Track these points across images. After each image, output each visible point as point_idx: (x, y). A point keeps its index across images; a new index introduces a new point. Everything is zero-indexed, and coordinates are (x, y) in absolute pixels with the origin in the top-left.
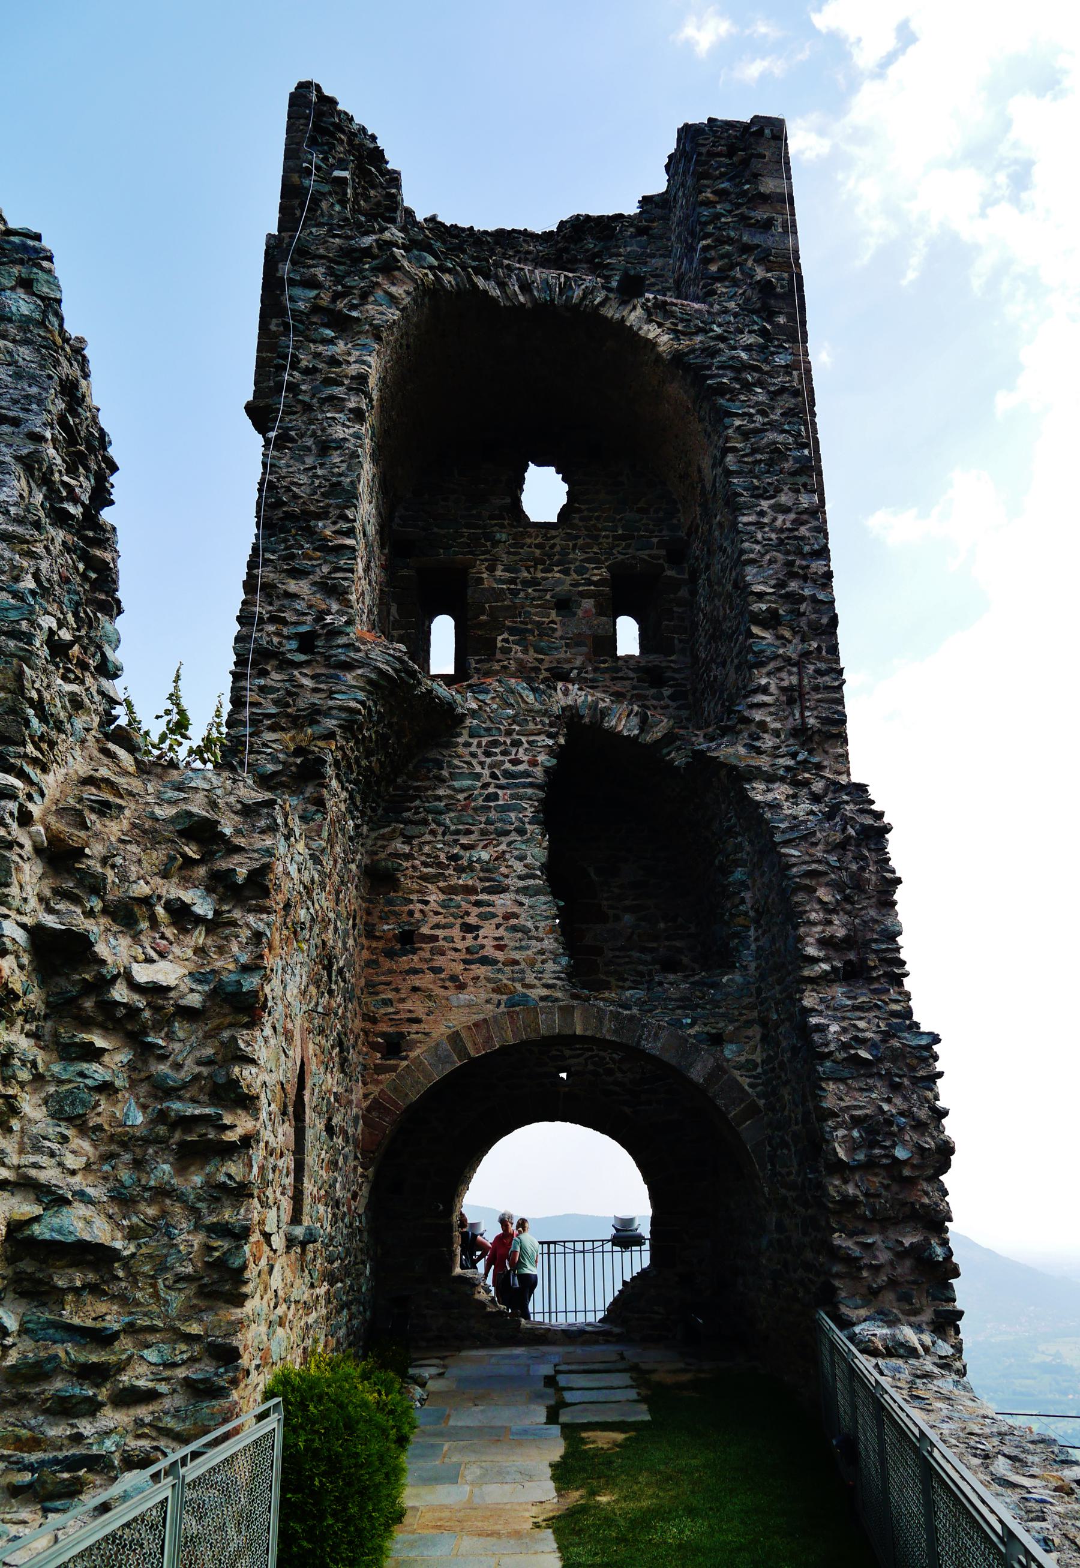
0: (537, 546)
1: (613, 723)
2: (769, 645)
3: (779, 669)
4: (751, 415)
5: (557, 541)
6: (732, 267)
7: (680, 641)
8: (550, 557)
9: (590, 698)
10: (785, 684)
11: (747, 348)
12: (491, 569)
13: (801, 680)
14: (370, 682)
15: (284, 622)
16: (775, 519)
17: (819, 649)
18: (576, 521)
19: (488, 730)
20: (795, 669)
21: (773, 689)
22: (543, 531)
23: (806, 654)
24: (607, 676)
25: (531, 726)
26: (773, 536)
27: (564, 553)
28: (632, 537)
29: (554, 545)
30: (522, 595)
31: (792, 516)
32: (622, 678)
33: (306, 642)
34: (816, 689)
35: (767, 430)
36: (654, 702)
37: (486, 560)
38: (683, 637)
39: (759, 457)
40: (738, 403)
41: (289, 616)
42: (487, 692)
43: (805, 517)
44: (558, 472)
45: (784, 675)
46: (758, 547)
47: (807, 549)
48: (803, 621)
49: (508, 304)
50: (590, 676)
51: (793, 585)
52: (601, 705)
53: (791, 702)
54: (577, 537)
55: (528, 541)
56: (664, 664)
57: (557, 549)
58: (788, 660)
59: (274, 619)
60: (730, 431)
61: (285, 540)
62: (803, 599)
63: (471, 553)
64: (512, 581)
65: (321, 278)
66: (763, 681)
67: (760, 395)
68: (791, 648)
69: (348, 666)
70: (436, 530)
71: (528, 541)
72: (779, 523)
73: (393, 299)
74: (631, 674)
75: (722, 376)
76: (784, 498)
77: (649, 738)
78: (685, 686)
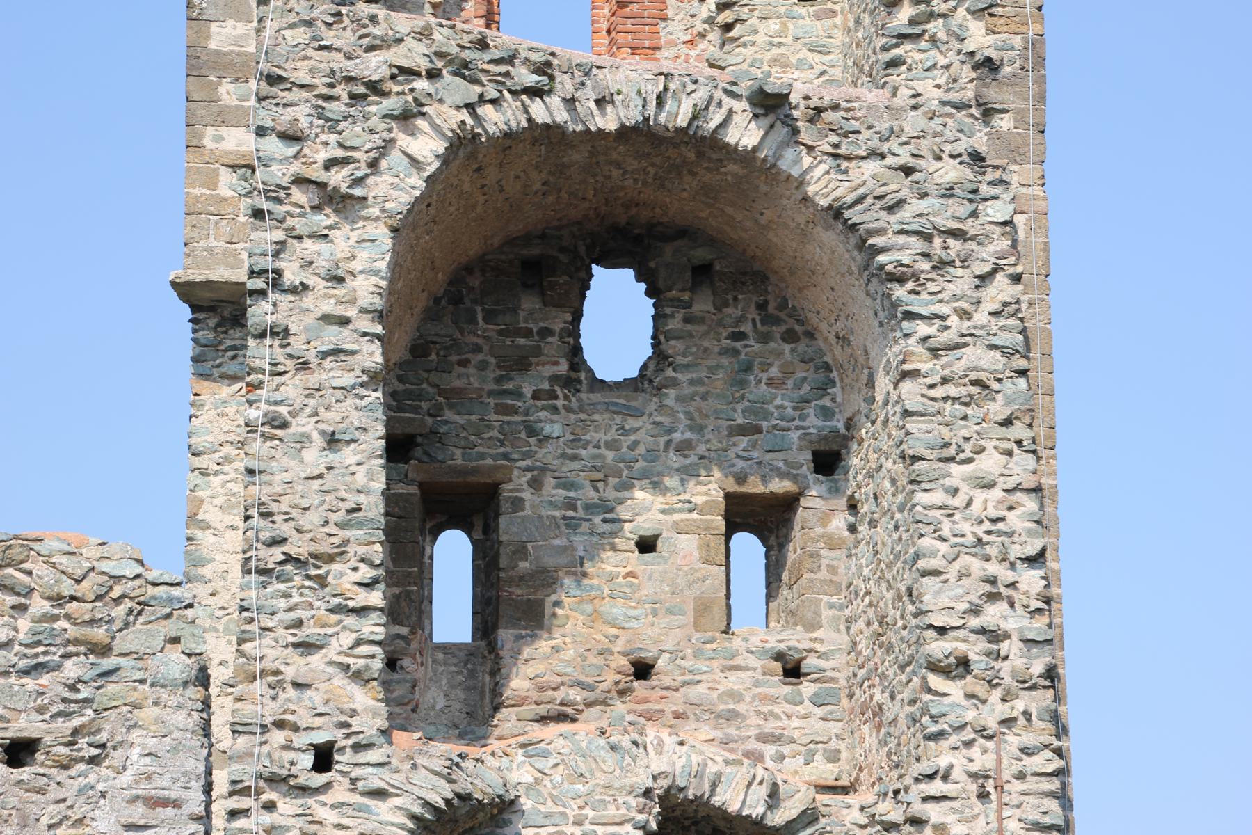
0: (611, 445)
1: (727, 796)
2: (953, 705)
3: (969, 744)
4: (943, 318)
5: (640, 436)
6: (931, 16)
7: (831, 606)
8: (629, 463)
9: (695, 759)
10: (974, 768)
11: (948, 192)
12: (536, 484)
13: (999, 761)
14: (414, 817)
15: (296, 728)
16: (969, 503)
17: (1027, 714)
18: (670, 402)
19: (548, 816)
20: (990, 745)
21: (956, 774)
22: (618, 419)
23: (1008, 722)
24: (716, 664)
25: (612, 810)
26: (966, 527)
27: (652, 456)
28: (758, 430)
29: (635, 444)
30: (585, 526)
31: (997, 493)
32: (738, 668)
33: (324, 758)
34: (1021, 776)
35: (966, 345)
36: (788, 708)
37: (528, 469)
38: (834, 599)
39: (952, 390)
40: (924, 296)
41: (304, 719)
42: (545, 755)
43: (1019, 496)
44: (638, 279)
45: (975, 752)
46: (943, 548)
47: (1016, 552)
48: (1005, 668)
49: (579, 128)
50: (687, 664)
51: (994, 614)
52: (712, 769)
53: (983, 796)
54: (670, 430)
55: (597, 436)
56: (806, 645)
57: (641, 449)
58: (981, 731)
59: (280, 724)
60: (912, 341)
61: (287, 596)
62: (1007, 636)
63: (506, 456)
64: (571, 504)
65: (304, 123)
66: (943, 762)
67: (961, 282)
68: (985, 709)
69: (380, 794)
70: (449, 415)
71: (597, 436)
72: (976, 507)
73: (413, 161)
74: (753, 661)
75: (901, 248)
76: (990, 463)
77: (778, 818)
78: (832, 680)
